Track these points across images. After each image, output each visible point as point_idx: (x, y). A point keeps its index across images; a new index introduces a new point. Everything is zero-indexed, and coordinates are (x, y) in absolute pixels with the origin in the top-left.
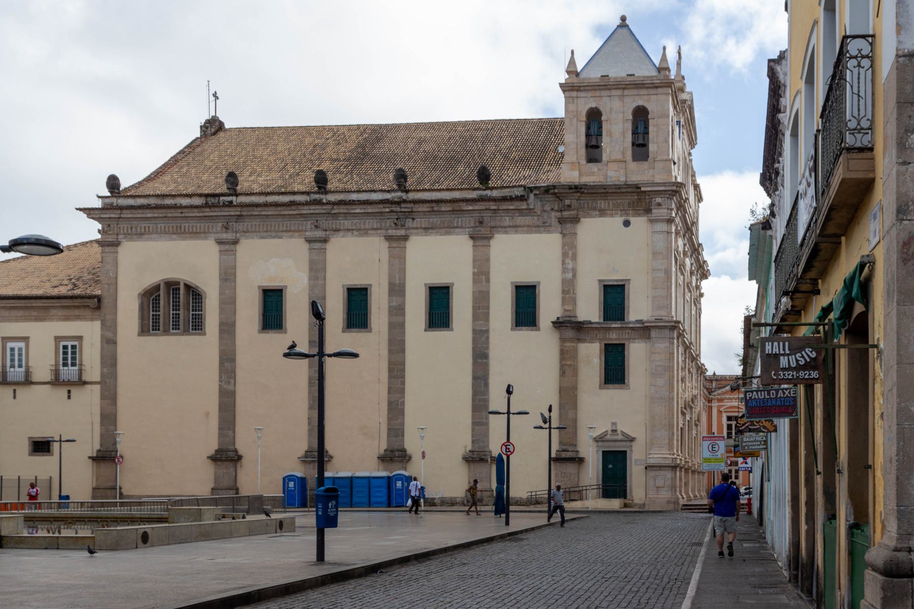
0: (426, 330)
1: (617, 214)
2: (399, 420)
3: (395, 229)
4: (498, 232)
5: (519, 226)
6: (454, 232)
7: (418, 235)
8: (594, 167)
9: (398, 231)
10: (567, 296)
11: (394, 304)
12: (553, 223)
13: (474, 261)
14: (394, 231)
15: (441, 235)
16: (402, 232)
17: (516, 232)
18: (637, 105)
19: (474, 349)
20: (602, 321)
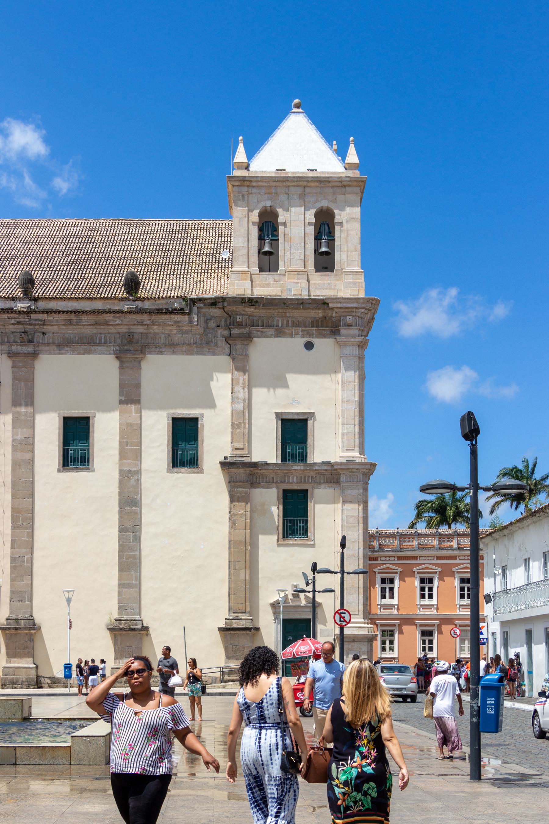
0: (59, 471)
1: (297, 334)
2: (25, 582)
3: (21, 345)
4: (150, 352)
5: (177, 345)
6: (95, 350)
7: (50, 353)
8: (268, 277)
9: (24, 348)
10: (238, 431)
11: (19, 437)
12: (219, 343)
13: (121, 386)
14: (20, 348)
15: (79, 353)
16: (30, 348)
17: (174, 353)
18: (321, 205)
19: (120, 493)
20: (279, 461)
